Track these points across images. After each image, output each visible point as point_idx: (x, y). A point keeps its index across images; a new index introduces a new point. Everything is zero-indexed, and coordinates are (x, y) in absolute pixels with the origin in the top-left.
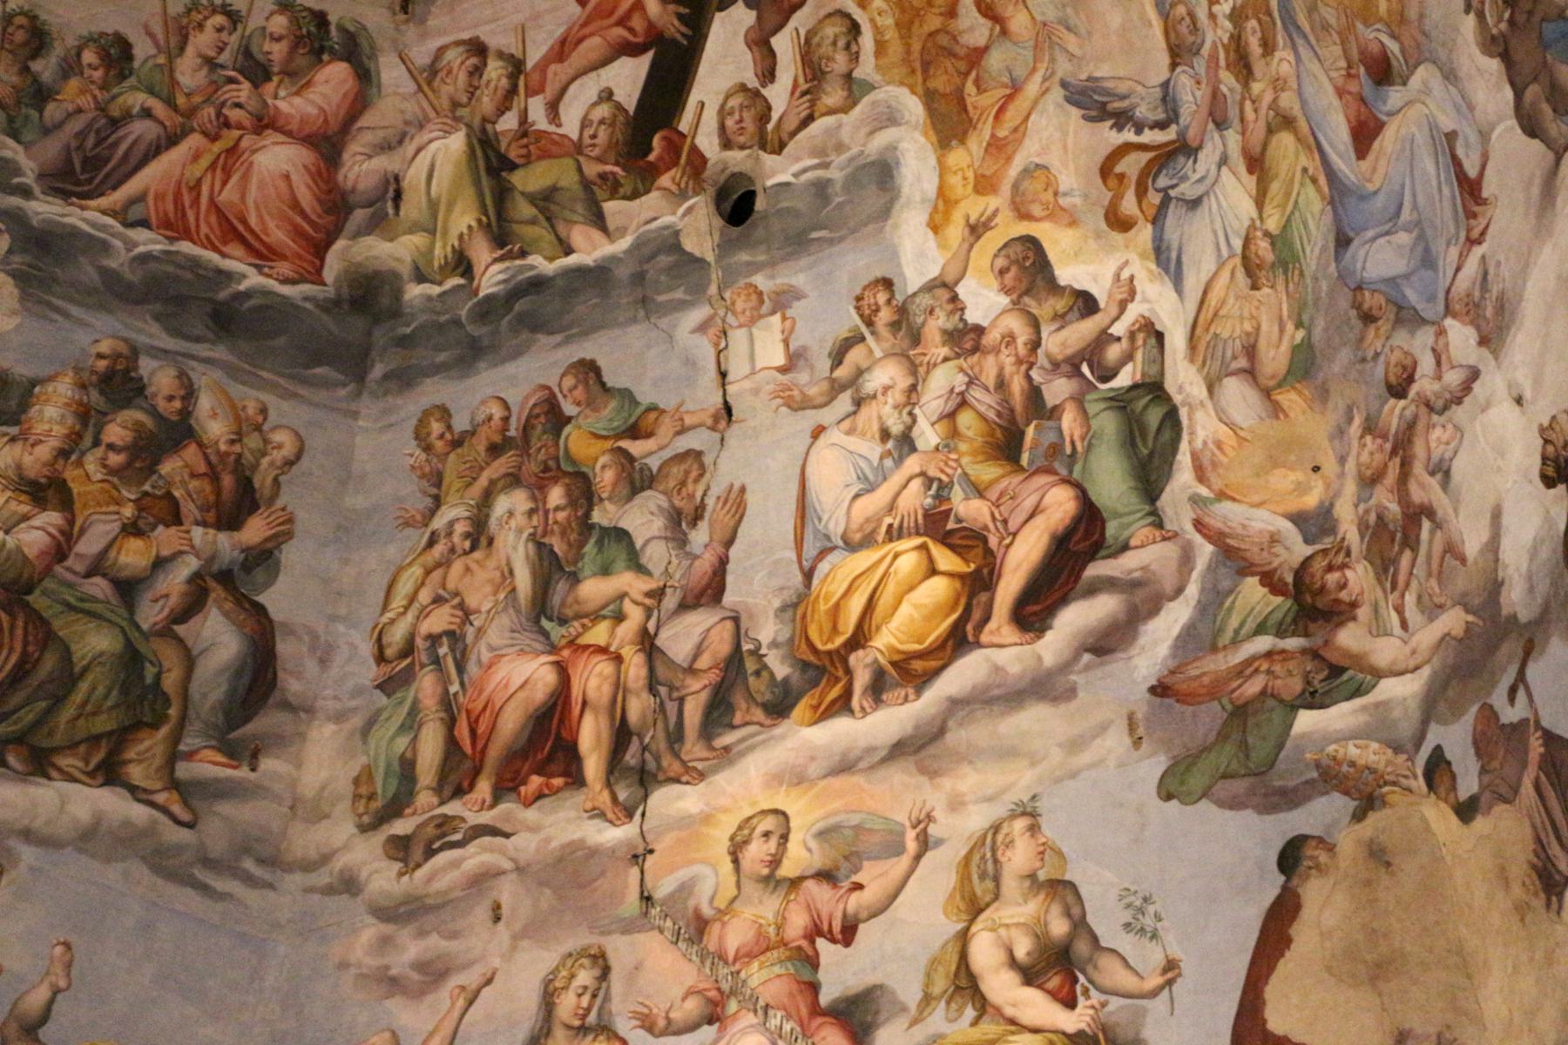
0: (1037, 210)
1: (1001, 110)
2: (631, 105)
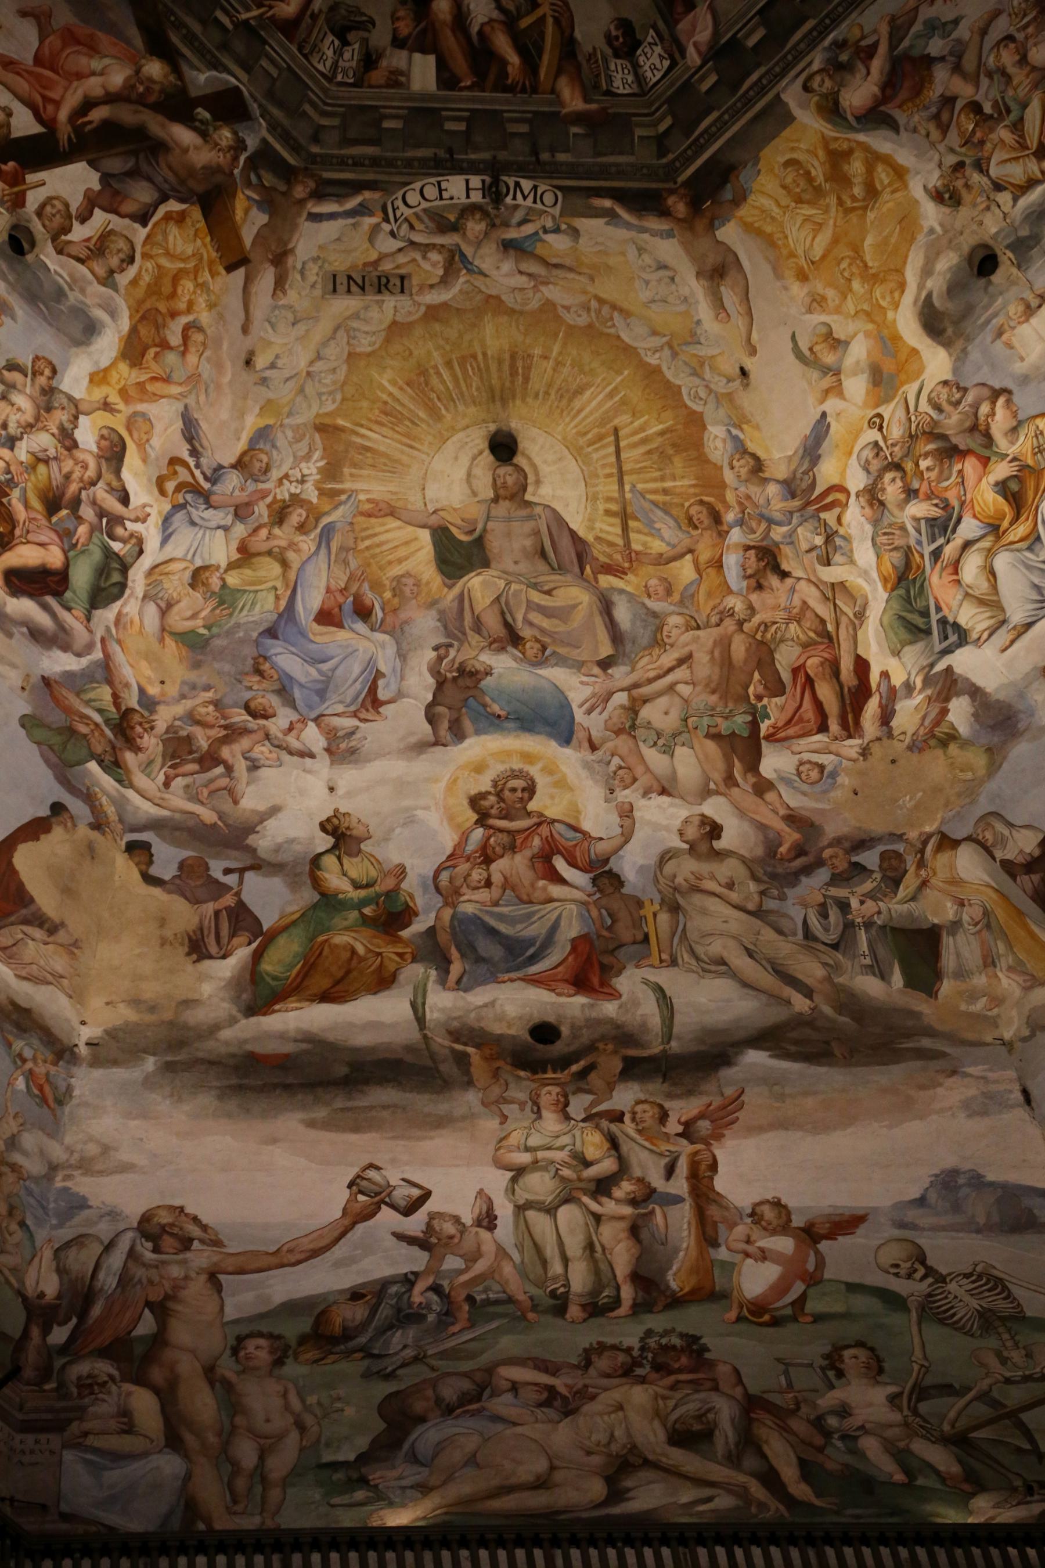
0: (136, 435)
1: (154, 379)
2: (16, 134)
